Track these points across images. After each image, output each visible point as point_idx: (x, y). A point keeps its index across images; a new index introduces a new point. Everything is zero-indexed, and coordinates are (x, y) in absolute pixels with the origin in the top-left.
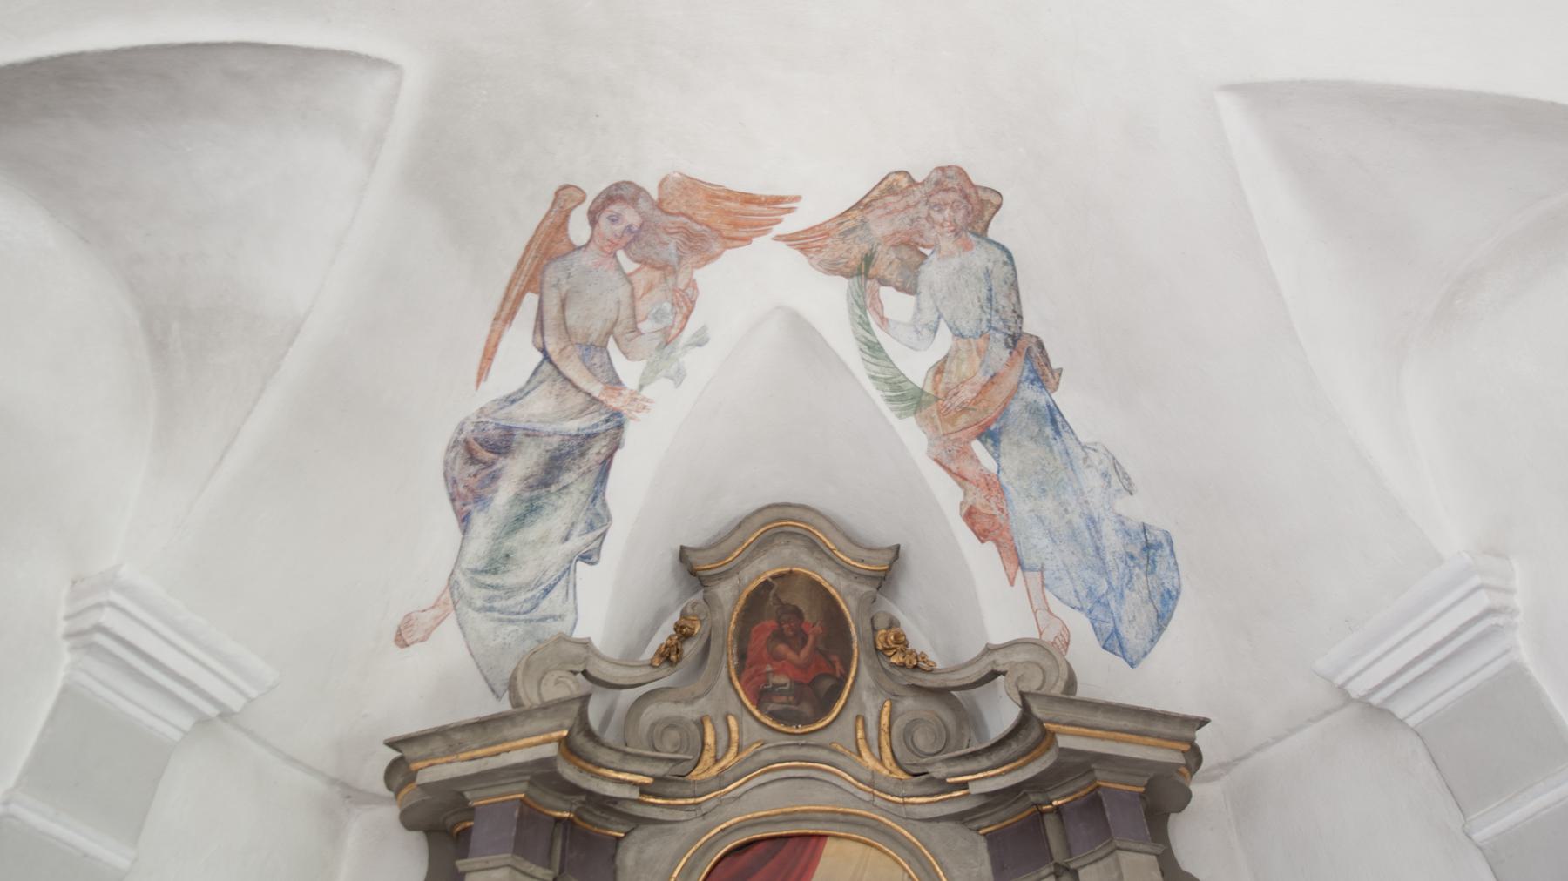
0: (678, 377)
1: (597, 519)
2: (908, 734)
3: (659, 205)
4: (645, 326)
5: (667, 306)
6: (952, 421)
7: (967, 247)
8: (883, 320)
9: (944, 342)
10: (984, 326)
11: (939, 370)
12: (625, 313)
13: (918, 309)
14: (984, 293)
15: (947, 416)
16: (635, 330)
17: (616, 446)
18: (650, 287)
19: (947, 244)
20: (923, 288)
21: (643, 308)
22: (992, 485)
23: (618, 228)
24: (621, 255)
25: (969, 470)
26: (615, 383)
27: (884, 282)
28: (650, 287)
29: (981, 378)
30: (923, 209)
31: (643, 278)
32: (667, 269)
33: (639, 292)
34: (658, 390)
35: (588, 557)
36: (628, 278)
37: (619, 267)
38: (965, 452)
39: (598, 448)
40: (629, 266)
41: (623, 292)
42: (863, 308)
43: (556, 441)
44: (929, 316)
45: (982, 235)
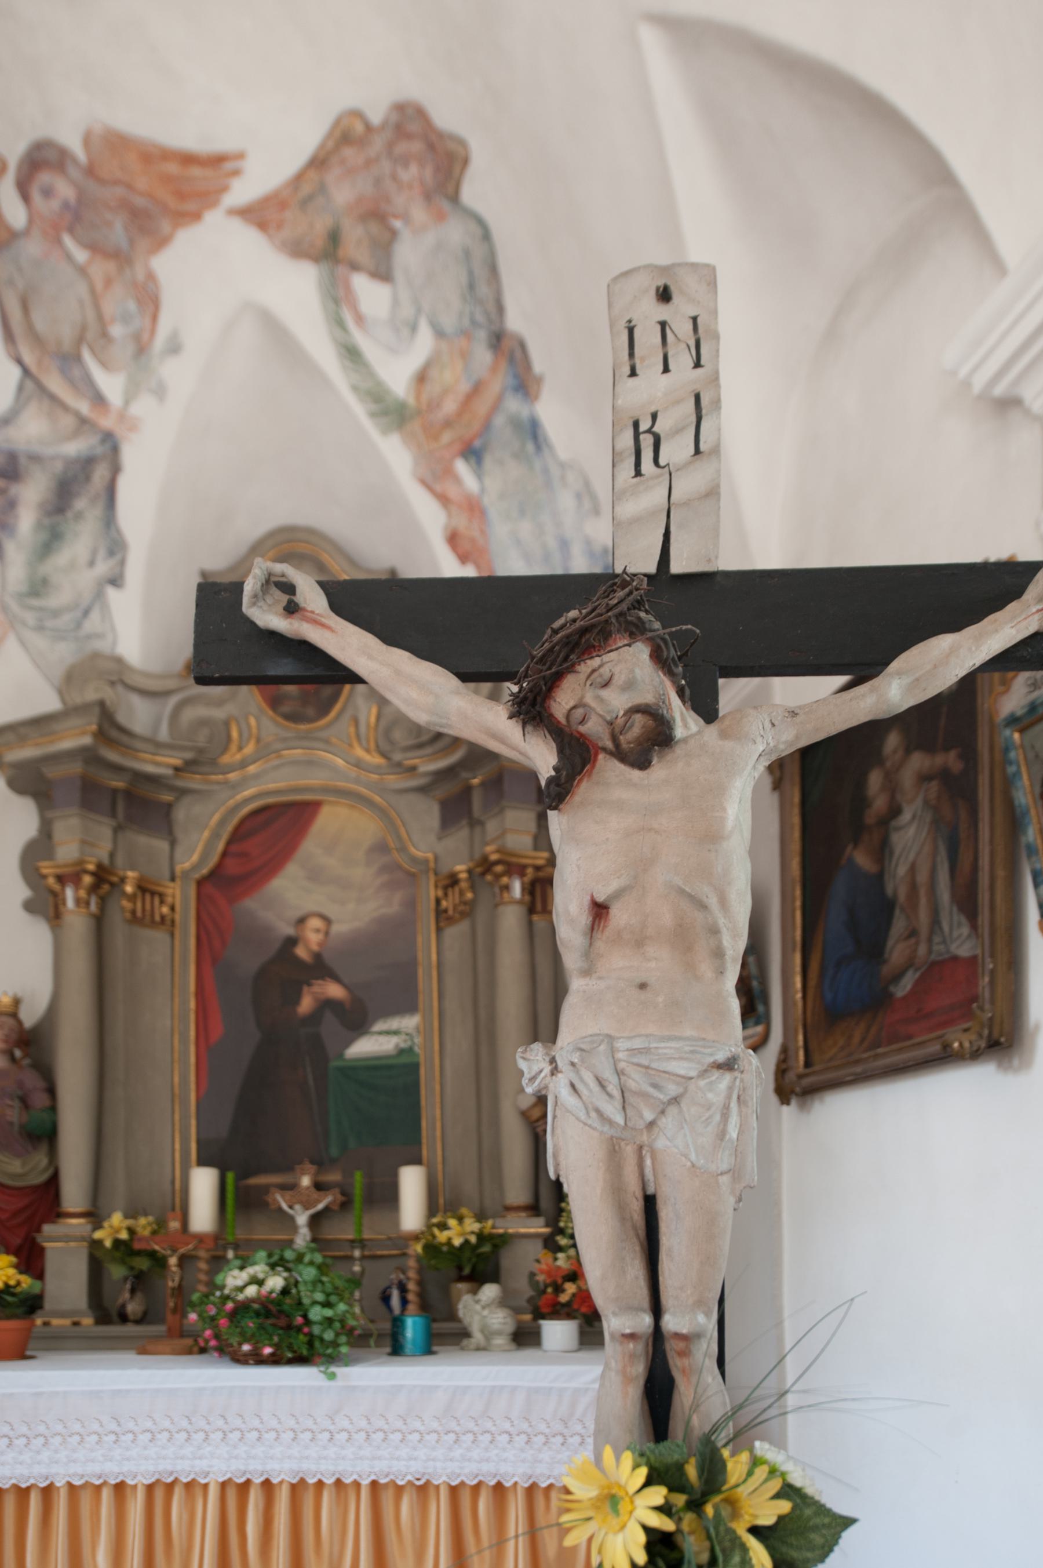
0: (160, 392)
1: (116, 547)
2: (387, 732)
3: (90, 171)
4: (117, 331)
5: (132, 306)
6: (436, 437)
7: (440, 217)
8: (360, 319)
9: (424, 344)
10: (466, 322)
11: (421, 378)
12: (90, 315)
13: (396, 302)
14: (464, 279)
15: (432, 433)
16: (104, 334)
17: (116, 469)
18: (108, 282)
19: (419, 213)
20: (398, 274)
21: (109, 308)
22: (474, 508)
23: (55, 204)
24: (68, 241)
25: (452, 492)
26: (99, 400)
27: (355, 267)
28: (108, 282)
29: (464, 387)
30: (386, 166)
31: (99, 270)
32: (121, 258)
33: (99, 286)
34: (143, 407)
35: (116, 581)
36: (82, 271)
37: (69, 257)
38: (448, 472)
39: (100, 474)
40: (81, 255)
41: (82, 289)
42: (336, 301)
43: (59, 466)
44: (407, 311)
45: (454, 198)
